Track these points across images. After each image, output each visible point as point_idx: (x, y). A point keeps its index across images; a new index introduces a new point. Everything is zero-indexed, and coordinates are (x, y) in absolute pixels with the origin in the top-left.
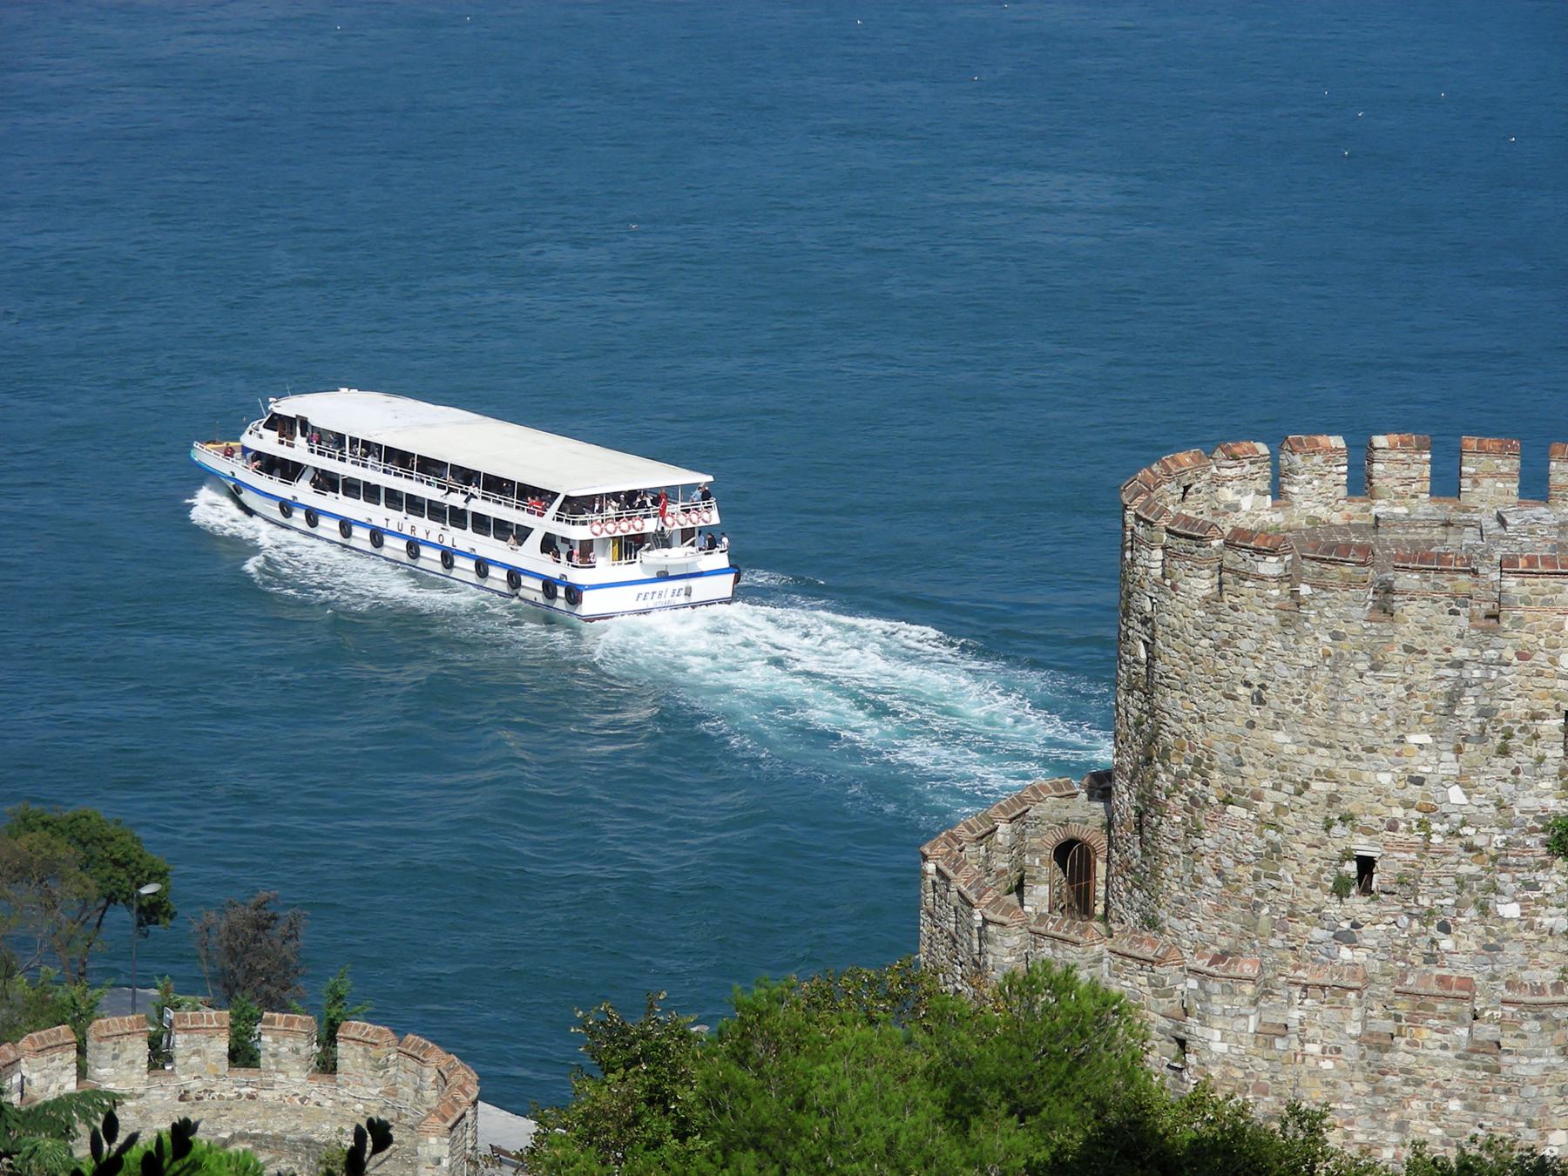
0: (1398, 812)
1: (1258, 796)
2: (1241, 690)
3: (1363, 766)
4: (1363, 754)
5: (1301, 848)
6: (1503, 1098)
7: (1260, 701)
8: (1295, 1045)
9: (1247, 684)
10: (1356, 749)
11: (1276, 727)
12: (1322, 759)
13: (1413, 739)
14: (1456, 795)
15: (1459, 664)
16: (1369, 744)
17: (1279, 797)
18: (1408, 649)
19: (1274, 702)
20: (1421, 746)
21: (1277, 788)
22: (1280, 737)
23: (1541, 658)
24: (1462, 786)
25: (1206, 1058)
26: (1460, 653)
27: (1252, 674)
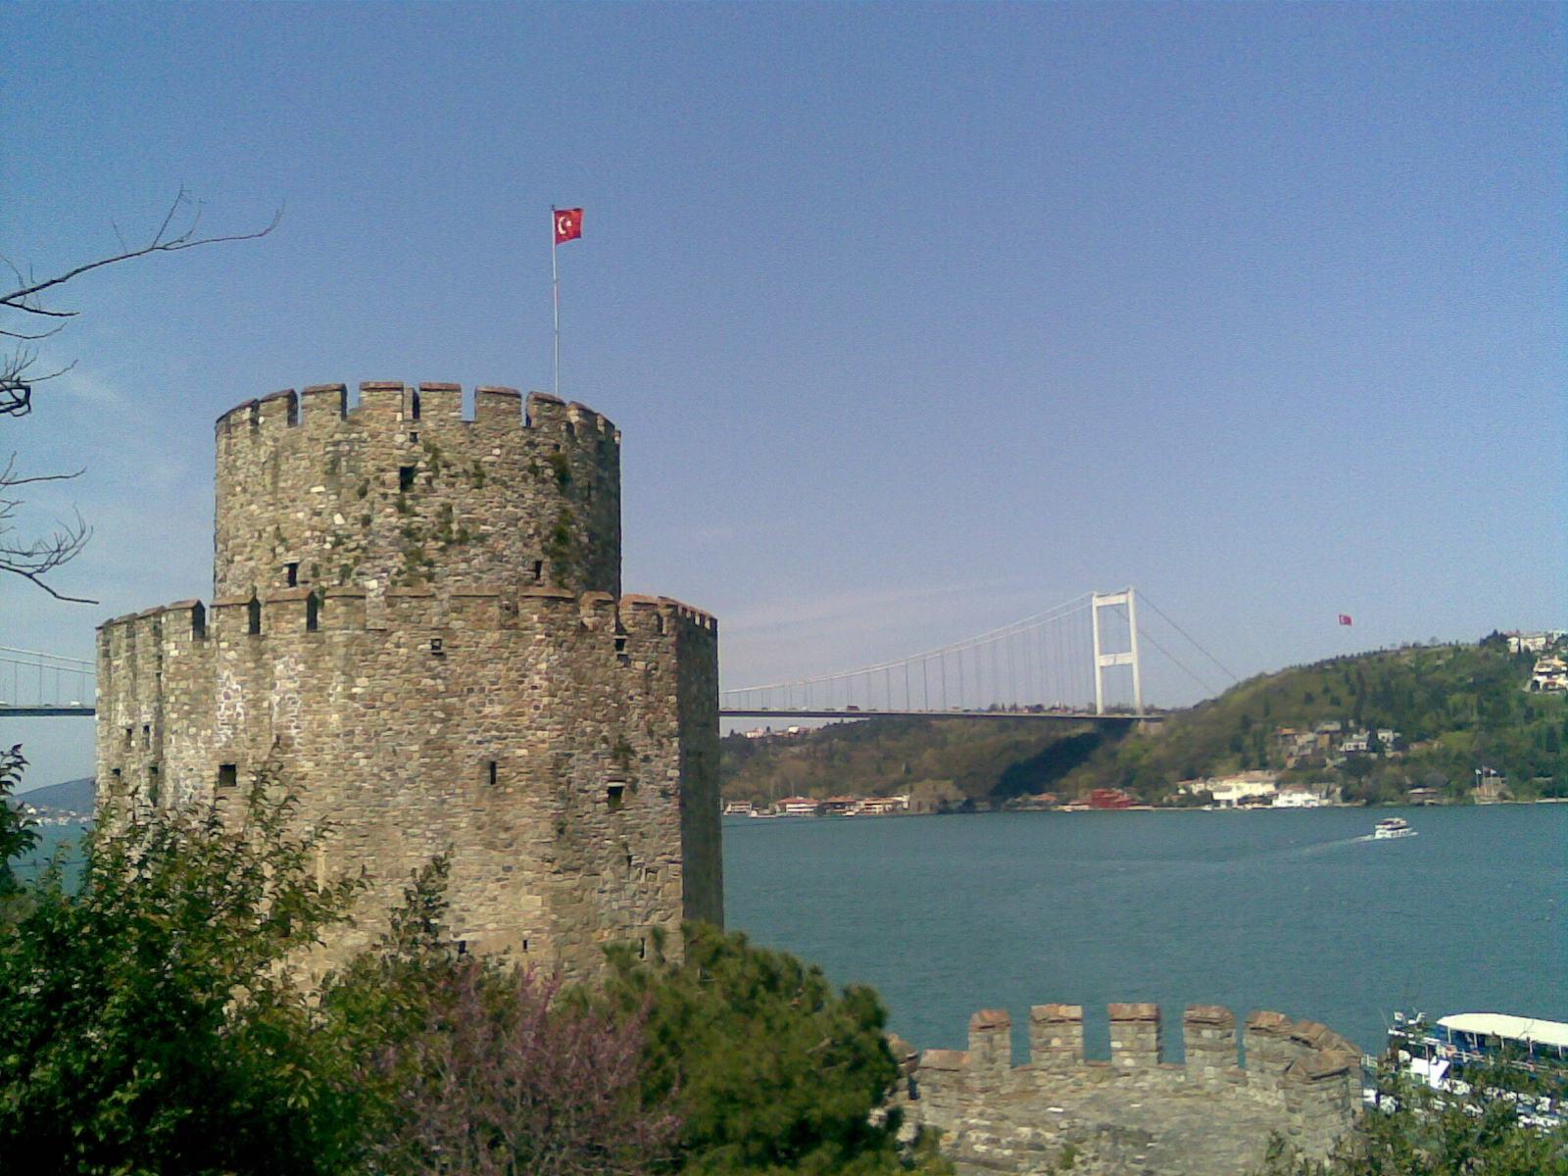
2: (238, 489)
3: (288, 511)
4: (290, 504)
6: (327, 658)
8: (214, 644)
10: (287, 502)
13: (315, 490)
14: (338, 519)
15: (337, 444)
16: (292, 496)
18: (310, 439)
19: (250, 490)
20: (319, 493)
22: (253, 507)
23: (383, 436)
24: (342, 514)
26: (338, 437)
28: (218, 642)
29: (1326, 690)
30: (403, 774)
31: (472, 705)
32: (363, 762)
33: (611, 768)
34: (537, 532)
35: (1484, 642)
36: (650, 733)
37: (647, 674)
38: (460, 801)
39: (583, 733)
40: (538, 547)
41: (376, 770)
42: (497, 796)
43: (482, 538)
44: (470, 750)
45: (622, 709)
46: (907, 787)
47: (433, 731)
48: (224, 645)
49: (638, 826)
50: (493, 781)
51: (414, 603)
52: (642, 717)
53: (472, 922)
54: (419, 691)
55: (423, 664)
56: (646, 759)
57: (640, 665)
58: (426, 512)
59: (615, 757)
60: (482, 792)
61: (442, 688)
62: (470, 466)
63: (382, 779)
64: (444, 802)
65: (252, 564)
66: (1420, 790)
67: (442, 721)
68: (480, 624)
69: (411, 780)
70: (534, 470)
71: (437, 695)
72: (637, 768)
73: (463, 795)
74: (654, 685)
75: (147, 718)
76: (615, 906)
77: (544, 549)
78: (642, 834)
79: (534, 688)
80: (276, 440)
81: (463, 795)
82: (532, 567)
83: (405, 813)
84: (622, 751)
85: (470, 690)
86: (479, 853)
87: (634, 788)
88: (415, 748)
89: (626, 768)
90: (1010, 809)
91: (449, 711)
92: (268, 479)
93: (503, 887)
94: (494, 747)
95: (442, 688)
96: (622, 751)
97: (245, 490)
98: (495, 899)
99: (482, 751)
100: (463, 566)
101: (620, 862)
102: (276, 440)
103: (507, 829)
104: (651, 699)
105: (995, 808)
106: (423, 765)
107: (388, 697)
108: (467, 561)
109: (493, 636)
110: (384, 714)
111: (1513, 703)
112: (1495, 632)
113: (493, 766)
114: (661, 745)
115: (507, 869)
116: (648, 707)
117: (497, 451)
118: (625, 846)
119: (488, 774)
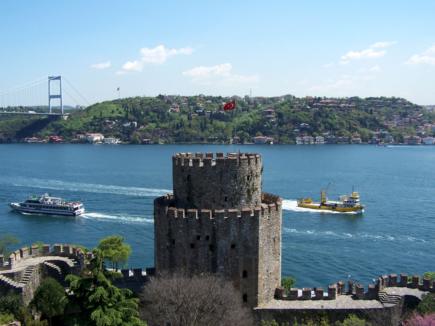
0: (230, 190)
1: (211, 191)
2: (207, 178)
5: (217, 197)
7: (210, 178)
9: (208, 177)
11: (213, 182)
12: (220, 185)
17: (213, 191)
21: (213, 190)
22: (214, 183)
25: (218, 223)
27: (209, 175)
28: (231, 219)
29: (117, 110)
30: (265, 243)
35: (157, 98)
48: (232, 220)
50: (274, 241)
65: (214, 196)
66: (146, 140)
75: (207, 233)
80: (221, 169)
90: (23, 142)
91: (270, 229)
92: (219, 178)
97: (210, 178)
102: (221, 169)
105: (18, 142)
111: (166, 115)
112: (160, 95)
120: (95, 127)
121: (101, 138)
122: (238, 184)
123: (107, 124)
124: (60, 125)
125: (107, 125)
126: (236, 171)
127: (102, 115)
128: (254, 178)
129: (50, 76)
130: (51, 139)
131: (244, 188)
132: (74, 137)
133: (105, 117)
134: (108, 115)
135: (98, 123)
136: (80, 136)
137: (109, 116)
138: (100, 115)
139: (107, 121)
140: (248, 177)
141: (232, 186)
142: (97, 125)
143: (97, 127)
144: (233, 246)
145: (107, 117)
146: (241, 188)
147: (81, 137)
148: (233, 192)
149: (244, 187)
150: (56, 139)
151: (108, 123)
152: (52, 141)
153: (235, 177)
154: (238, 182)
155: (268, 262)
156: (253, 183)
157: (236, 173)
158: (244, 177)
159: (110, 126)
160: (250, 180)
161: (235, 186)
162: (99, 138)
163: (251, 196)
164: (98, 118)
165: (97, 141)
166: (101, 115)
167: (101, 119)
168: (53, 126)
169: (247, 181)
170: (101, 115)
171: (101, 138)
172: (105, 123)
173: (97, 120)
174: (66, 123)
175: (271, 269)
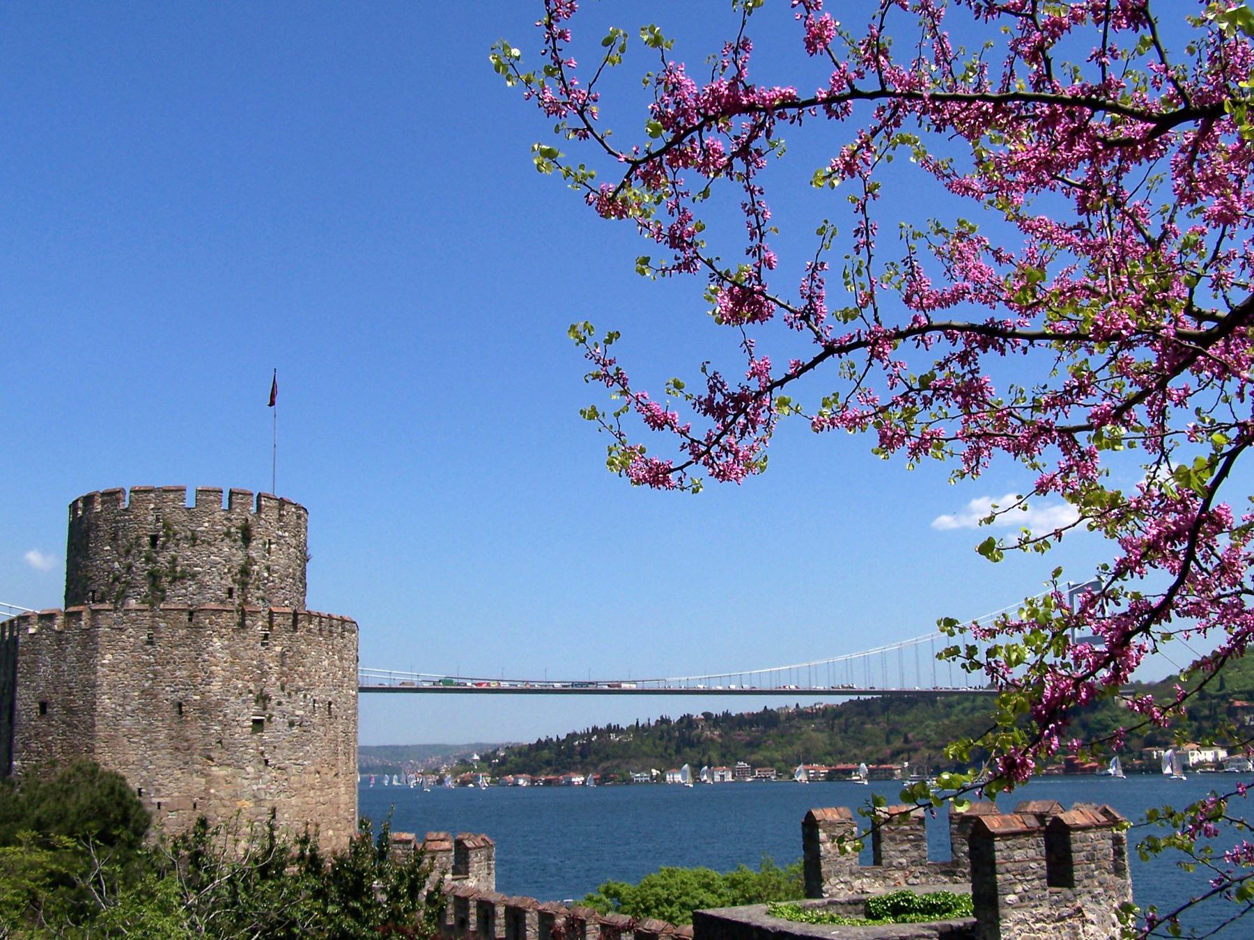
14: (116, 565)
30: (129, 708)
31: (169, 671)
32: (108, 701)
33: (255, 708)
34: (229, 571)
36: (283, 689)
37: (283, 654)
38: (160, 724)
39: (236, 688)
40: (230, 579)
41: (113, 706)
42: (181, 722)
43: (194, 576)
44: (167, 694)
45: (264, 674)
46: (905, 755)
47: (147, 685)
49: (272, 742)
50: (181, 712)
51: (139, 613)
52: (278, 679)
53: (164, 792)
54: (139, 663)
55: (142, 647)
56: (280, 703)
57: (278, 649)
58: (163, 560)
59: (257, 701)
60: (173, 718)
61: (153, 661)
62: (189, 533)
63: (116, 711)
64: (152, 724)
67: (152, 679)
68: (174, 626)
69: (133, 711)
70: (228, 534)
71: (150, 664)
72: (273, 709)
73: (163, 720)
74: (288, 661)
76: (255, 787)
77: (234, 581)
78: (275, 747)
79: (205, 661)
81: (163, 720)
82: (226, 591)
83: (130, 729)
84: (263, 699)
85: (168, 663)
86: (170, 753)
87: (269, 719)
88: (136, 694)
89: (265, 709)
91: (155, 673)
93: (183, 773)
94: (181, 694)
95: (153, 661)
96: (263, 699)
98: (178, 779)
99: (174, 696)
100: (184, 591)
101: (260, 762)
103: (187, 741)
104: (285, 669)
106: (140, 703)
107: (123, 666)
108: (186, 589)
109: (182, 632)
110: (120, 675)
113: (180, 705)
114: (289, 694)
115: (186, 763)
116: (283, 673)
117: (206, 524)
118: (262, 753)
119: (177, 709)
120: (1200, 724)
121: (1216, 754)
122: (120, 556)
123: (1239, 711)
124: (1099, 722)
125: (1239, 717)
126: (117, 522)
127: (1227, 685)
128: (177, 545)
129: (1072, 583)
130: (1070, 764)
131: (137, 568)
132: (1136, 754)
133: (1235, 693)
134: (1245, 686)
135: (1210, 710)
136: (1151, 753)
137: (1247, 688)
138: (1218, 687)
139: (1238, 704)
140: (154, 539)
141: (106, 562)
142: (1206, 718)
143: (1206, 724)
144: (43, 707)
145: (1241, 692)
146: (129, 567)
147: (1155, 753)
148: (108, 576)
149: (139, 565)
150: (1083, 764)
151: (1243, 708)
152: (1071, 769)
153: (115, 538)
154: (122, 550)
155: (146, 769)
156: (174, 559)
157: (117, 529)
158: (138, 538)
159: (1247, 718)
160: (162, 548)
161: (113, 562)
162: (1208, 755)
163: (163, 591)
164: (1214, 697)
165: (1200, 764)
166: (1222, 687)
167: (1224, 697)
168: (1084, 726)
169: (147, 548)
170: (1222, 687)
171: (1216, 754)
172: (1232, 712)
173: (1207, 702)
174: (1116, 716)
175: (158, 790)
